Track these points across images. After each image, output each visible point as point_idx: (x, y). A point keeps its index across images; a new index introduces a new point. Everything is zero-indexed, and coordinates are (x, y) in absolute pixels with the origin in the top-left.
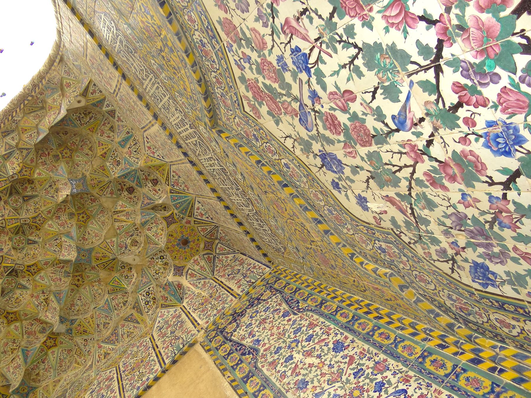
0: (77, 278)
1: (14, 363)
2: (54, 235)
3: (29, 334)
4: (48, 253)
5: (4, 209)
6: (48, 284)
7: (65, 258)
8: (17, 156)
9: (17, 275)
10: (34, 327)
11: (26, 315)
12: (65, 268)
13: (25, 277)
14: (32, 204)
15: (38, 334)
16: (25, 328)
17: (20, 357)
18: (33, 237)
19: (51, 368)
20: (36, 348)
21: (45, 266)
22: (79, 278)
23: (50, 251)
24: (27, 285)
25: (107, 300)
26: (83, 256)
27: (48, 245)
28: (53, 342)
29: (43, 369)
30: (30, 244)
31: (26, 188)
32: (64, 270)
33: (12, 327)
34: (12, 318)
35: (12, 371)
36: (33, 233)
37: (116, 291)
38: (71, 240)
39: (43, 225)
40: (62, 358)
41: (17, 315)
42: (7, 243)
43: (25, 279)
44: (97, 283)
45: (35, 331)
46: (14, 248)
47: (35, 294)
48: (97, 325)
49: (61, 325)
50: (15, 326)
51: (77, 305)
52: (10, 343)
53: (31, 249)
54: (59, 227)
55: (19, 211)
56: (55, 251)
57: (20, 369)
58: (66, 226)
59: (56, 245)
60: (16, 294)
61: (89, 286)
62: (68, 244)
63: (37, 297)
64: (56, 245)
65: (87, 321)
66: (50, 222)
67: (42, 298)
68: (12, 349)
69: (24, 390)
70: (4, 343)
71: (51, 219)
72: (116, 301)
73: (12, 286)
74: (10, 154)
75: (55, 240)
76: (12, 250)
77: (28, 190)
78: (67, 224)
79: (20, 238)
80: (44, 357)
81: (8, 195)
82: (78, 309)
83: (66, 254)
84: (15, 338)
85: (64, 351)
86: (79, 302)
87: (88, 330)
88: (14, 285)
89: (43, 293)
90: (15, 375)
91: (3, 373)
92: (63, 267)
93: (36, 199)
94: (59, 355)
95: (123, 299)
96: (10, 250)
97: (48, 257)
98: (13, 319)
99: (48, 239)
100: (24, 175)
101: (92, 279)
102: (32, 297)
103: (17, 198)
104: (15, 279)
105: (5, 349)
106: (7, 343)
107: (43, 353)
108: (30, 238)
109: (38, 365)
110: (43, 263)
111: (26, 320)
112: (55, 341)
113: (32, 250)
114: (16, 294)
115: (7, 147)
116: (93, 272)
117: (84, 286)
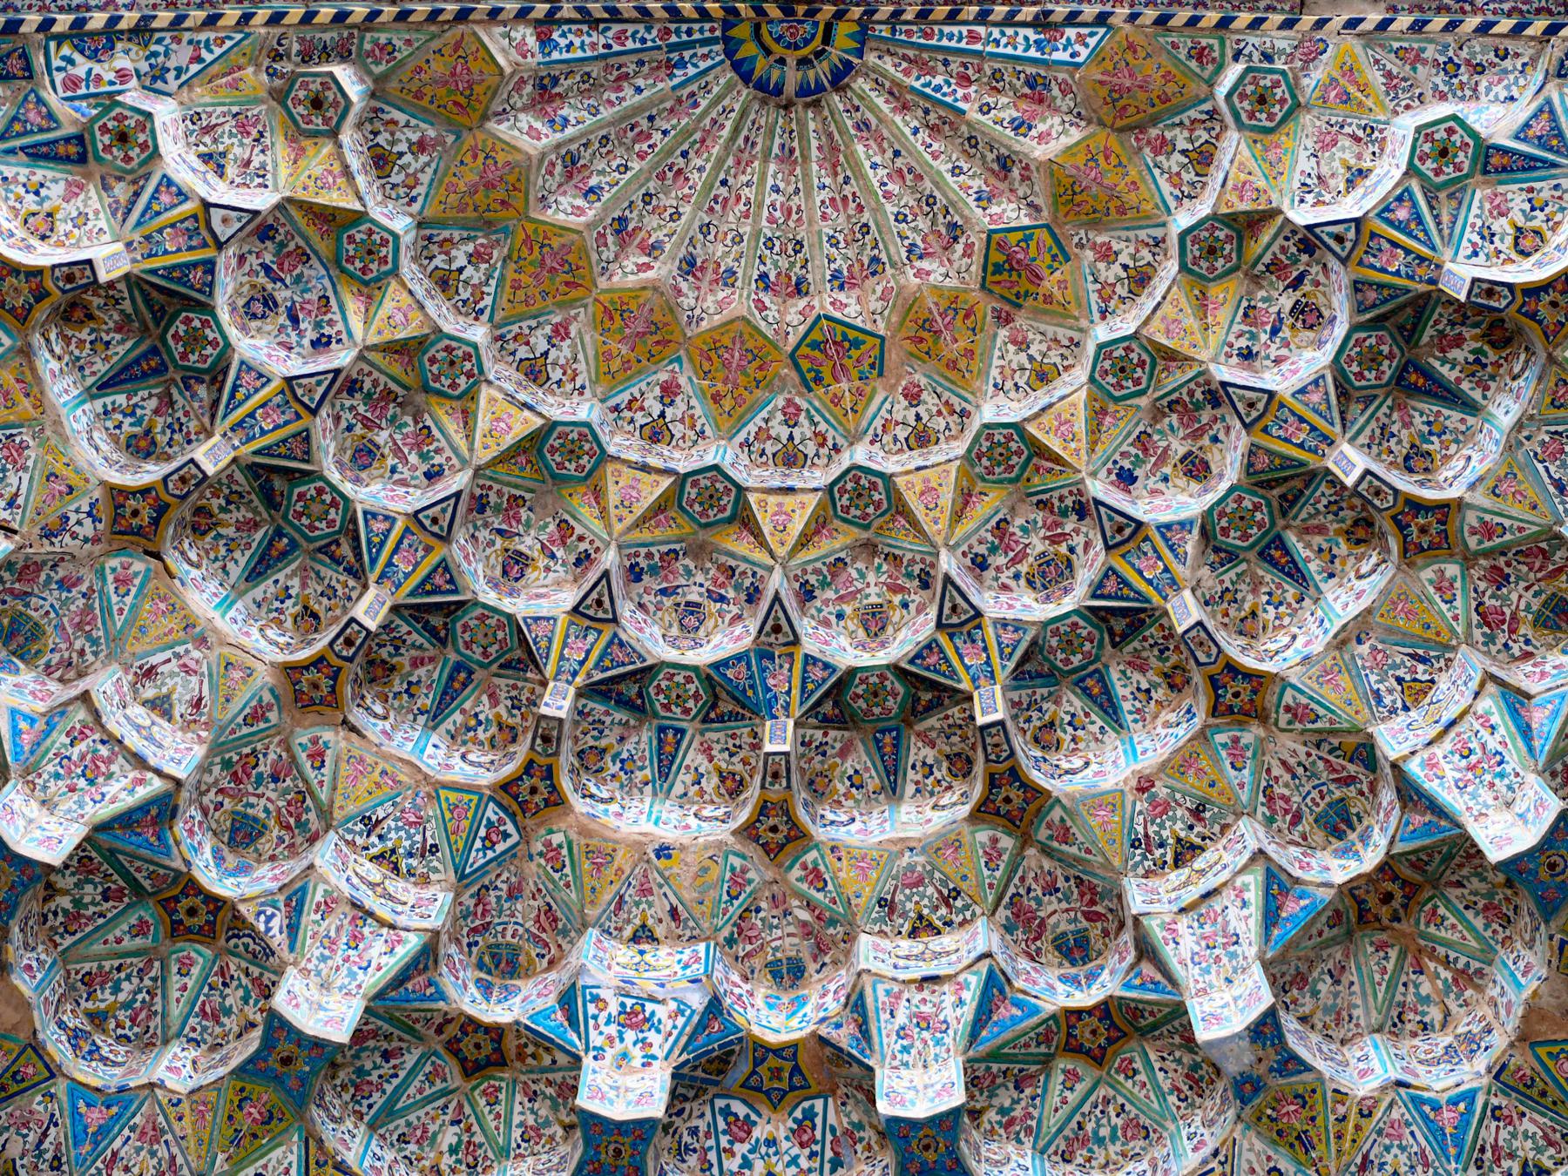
0: (1389, 886)
1: (926, 994)
2: (1430, 634)
3: (1017, 916)
4: (1344, 680)
5: (1275, 332)
6: (1244, 796)
7: (1432, 786)
8: (1546, 194)
9: (1124, 636)
10: (1052, 903)
11: (1065, 836)
12: (1352, 791)
13: (1143, 670)
14: (1418, 420)
15: (1045, 944)
16: (1022, 879)
17: (967, 995)
18: (1308, 546)
19: (1028, 1131)
20: (1037, 1010)
21: (1284, 718)
22: (1398, 894)
23: (1356, 677)
24: (1127, 706)
25: (1470, 1096)
26: (1552, 866)
27: (1364, 649)
28: (1102, 1041)
29: (1002, 1111)
30: (1273, 563)
31: (1458, 342)
32: (1338, 794)
33: (983, 836)
34: (1007, 800)
35: (902, 1018)
36: (1321, 530)
37: (1534, 1093)
38: (1520, 743)
39: (1419, 561)
40: (1090, 1127)
41: (1033, 807)
42: (1167, 470)
43: (1136, 676)
44: (1446, 974)
45: (1042, 924)
46: (1204, 533)
47: (1161, 791)
48: (1365, 1157)
49: (1245, 1043)
50: (995, 841)
51: (1315, 994)
52: (930, 890)
53: (1256, 586)
54: (1475, 618)
55: (1355, 409)
56: (1377, 693)
57: (938, 1042)
58: (1502, 638)
59: (1399, 680)
60: (1057, 703)
61: (1402, 955)
62: (1493, 744)
63: (1161, 809)
64: (1399, 680)
65: (1341, 1110)
66: (1452, 570)
67: (1176, 826)
68: (921, 917)
69: (927, 1148)
70: (911, 868)
71: (1468, 560)
72: (1504, 1134)
73: (1067, 661)
74: (1530, 164)
75: (1413, 656)
76: (1196, 531)
77: (1456, 354)
78: (1512, 631)
79: (1257, 507)
80: (1034, 1068)
81: (1368, 316)
82: (1307, 1010)
83: (1451, 775)
84: (964, 886)
85: (1111, 1110)
86: (1325, 987)
87: (1321, 1147)
88: (1076, 660)
89: (1197, 813)
90: (905, 1049)
91: (869, 1000)
92: (1349, 781)
93: (1456, 415)
94: (1086, 1108)
95: (1538, 1150)
96: (1185, 525)
97: (1332, 696)
98: (1004, 809)
99: (1389, 630)
100: (1532, 316)
101: (1448, 944)
102: (1141, 790)
103: (1385, 349)
104: (1101, 646)
105: (899, 897)
106: (920, 882)
107: (1043, 1049)
108: (1291, 538)
109: (999, 1080)
110: (1288, 698)
111: (1046, 851)
112: (1110, 1041)
113: (1254, 591)
114: (1057, 703)
115: (1538, 128)
116: (1479, 923)
117: (1384, 936)
